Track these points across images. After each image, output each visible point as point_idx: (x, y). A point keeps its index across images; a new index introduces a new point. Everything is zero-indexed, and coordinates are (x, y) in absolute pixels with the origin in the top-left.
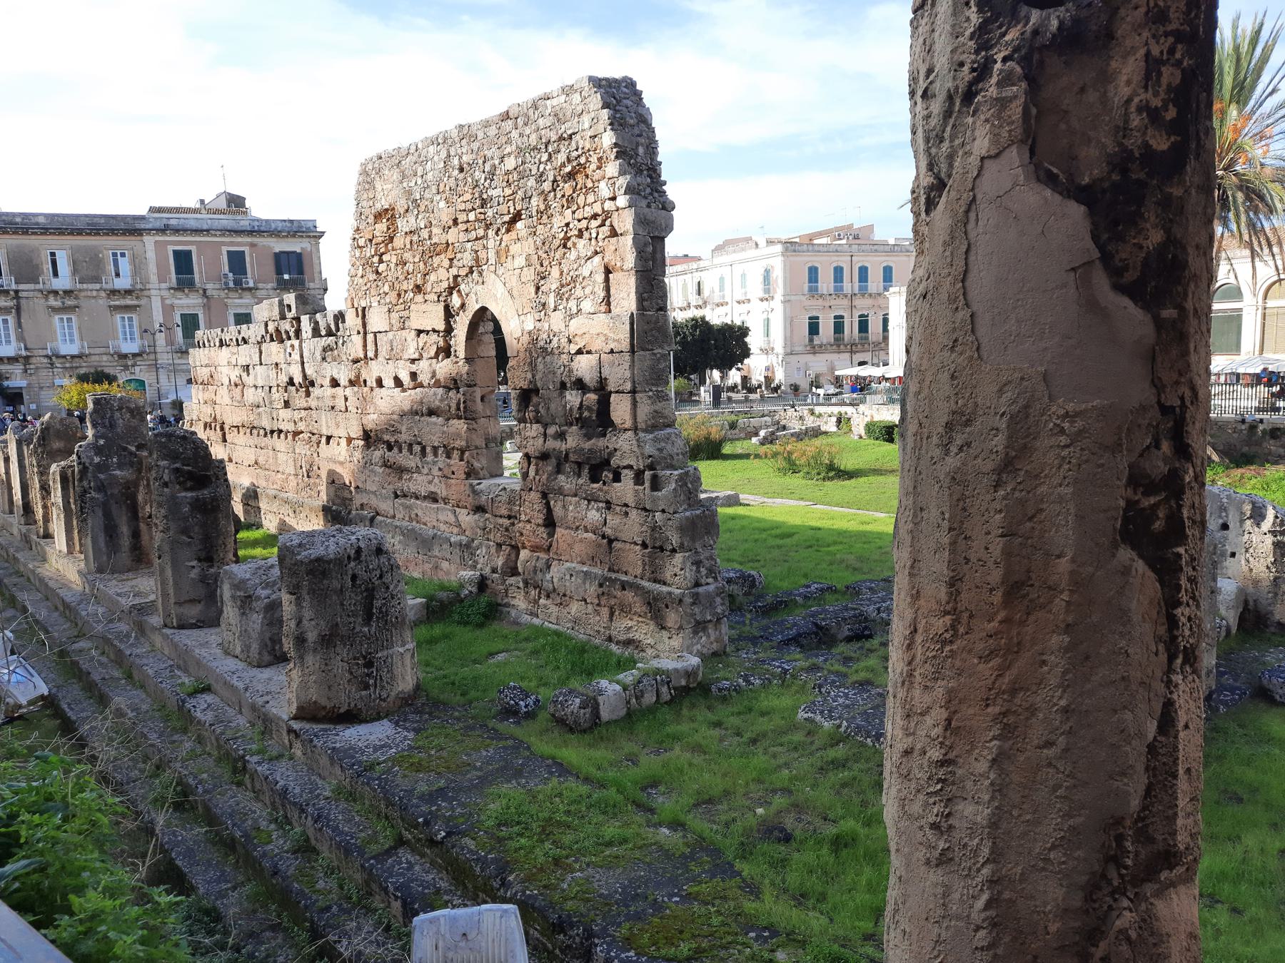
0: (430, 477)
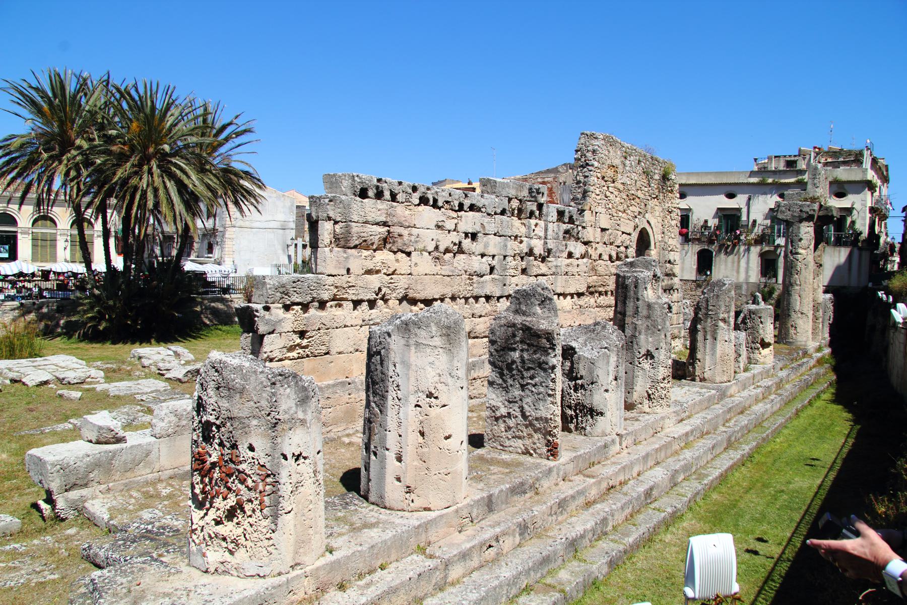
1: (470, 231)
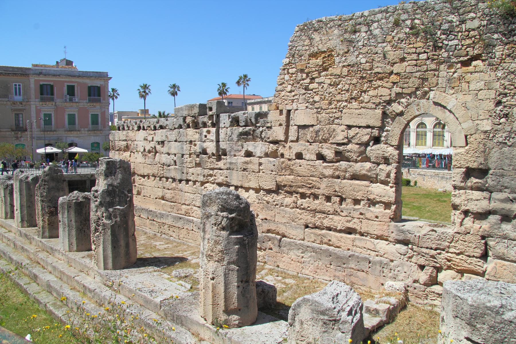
0: (350, 218)
1: (160, 140)
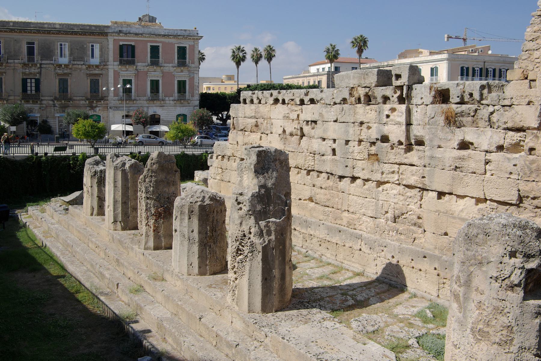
1: (310, 120)
